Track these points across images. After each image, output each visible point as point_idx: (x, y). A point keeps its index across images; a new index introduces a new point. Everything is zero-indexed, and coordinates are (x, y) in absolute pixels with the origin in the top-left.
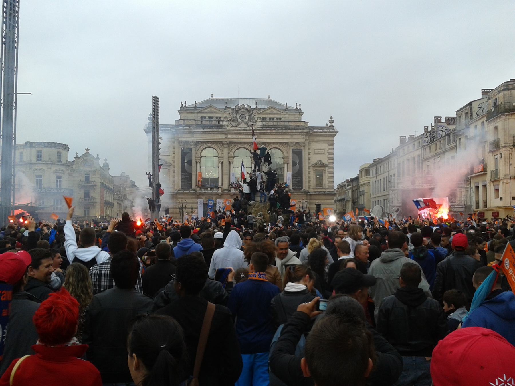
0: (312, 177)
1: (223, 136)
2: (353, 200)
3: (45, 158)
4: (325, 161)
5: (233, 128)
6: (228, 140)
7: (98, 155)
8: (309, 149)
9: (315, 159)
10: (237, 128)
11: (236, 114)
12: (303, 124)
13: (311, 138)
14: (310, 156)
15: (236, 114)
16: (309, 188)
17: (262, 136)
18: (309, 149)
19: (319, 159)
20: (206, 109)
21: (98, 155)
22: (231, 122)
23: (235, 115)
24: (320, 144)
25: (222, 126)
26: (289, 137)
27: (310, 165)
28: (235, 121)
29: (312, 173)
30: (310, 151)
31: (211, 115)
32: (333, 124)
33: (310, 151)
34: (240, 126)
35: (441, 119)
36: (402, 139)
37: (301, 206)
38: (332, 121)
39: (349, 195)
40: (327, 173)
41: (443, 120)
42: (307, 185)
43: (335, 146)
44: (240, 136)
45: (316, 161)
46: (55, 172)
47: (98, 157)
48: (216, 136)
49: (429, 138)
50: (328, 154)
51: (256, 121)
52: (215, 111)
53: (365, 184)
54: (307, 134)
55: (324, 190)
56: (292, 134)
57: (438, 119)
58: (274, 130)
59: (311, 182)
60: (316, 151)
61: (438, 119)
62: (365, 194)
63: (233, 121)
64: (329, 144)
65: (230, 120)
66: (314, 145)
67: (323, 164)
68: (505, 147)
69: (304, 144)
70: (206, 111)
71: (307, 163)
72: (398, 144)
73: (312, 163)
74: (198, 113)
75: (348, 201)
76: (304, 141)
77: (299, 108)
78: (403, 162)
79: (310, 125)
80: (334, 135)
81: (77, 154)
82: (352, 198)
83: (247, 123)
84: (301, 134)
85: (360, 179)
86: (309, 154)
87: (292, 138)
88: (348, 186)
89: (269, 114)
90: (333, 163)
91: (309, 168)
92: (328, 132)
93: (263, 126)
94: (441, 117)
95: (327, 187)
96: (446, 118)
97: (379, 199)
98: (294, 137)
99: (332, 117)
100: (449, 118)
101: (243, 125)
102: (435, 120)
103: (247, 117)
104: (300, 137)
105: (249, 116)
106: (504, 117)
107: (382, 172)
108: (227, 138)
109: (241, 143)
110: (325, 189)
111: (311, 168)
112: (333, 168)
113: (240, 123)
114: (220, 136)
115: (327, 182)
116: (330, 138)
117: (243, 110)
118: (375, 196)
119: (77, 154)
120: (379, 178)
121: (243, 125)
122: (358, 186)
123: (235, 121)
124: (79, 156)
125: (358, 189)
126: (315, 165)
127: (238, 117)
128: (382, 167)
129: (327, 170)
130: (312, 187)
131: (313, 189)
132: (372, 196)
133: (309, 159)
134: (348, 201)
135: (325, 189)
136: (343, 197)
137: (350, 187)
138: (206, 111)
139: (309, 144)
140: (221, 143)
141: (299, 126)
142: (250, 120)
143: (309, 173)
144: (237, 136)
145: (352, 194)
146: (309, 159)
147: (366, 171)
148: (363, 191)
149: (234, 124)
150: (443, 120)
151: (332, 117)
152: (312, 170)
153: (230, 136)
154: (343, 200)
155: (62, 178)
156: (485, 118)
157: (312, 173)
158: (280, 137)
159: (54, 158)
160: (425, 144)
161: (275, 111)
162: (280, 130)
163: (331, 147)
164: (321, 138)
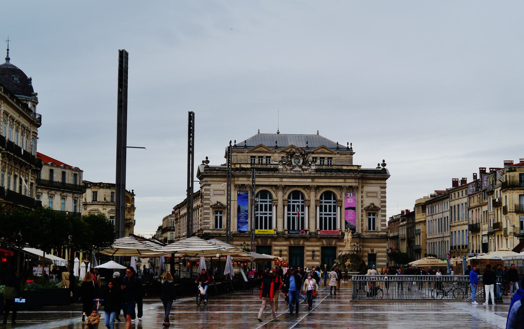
0: (364, 220)
1: (278, 180)
2: (408, 239)
3: (100, 198)
4: (377, 204)
5: (288, 172)
6: (283, 184)
7: (133, 191)
8: (362, 193)
9: (367, 202)
10: (292, 172)
11: (291, 158)
12: (356, 168)
13: (364, 181)
14: (363, 199)
15: (291, 158)
16: (362, 230)
17: (316, 180)
18: (362, 193)
19: (372, 202)
20: (256, 148)
21: (133, 191)
22: (286, 166)
23: (289, 159)
24: (372, 188)
25: (276, 170)
26: (342, 180)
27: (363, 208)
28: (290, 164)
29: (364, 216)
30: (363, 195)
31: (261, 155)
32: (385, 167)
33: (363, 195)
34: (295, 169)
35: (485, 170)
36: (455, 183)
37: (356, 249)
38: (384, 165)
39: (403, 232)
40: (379, 216)
41: (488, 171)
42: (360, 228)
43: (387, 190)
44: (295, 180)
45: (368, 205)
47: (133, 193)
48: (271, 180)
49: (474, 188)
50: (380, 197)
51: (310, 165)
52: (265, 150)
53: (420, 222)
54: (359, 178)
55: (377, 234)
56: (345, 178)
57: (482, 171)
58: (329, 174)
59: (364, 225)
60: (369, 194)
61: (482, 171)
62: (421, 233)
63: (288, 165)
64: (382, 188)
65: (285, 164)
66: (367, 189)
67: (376, 207)
68: (510, 212)
69: (357, 188)
70: (256, 150)
71: (360, 206)
72: (450, 186)
73: (365, 206)
74: (248, 153)
75: (403, 240)
76: (357, 184)
77: (350, 147)
78: (455, 206)
79: (362, 168)
82: (407, 236)
83: (300, 167)
84: (355, 178)
85: (416, 215)
86: (362, 197)
87: (345, 182)
88: (402, 221)
89: (320, 153)
90: (385, 206)
91: (362, 212)
92: (380, 175)
93: (317, 170)
94: (485, 168)
95: (380, 230)
96: (490, 169)
97: (435, 240)
98: (348, 181)
99: (384, 161)
100: (493, 169)
101: (297, 169)
102: (480, 171)
103: (301, 161)
104: (353, 181)
105: (303, 159)
106: (509, 191)
107: (437, 212)
108: (282, 181)
109: (295, 186)
110: (378, 232)
111: (364, 211)
112: (385, 211)
113: (294, 167)
114: (275, 180)
115: (380, 225)
116: (383, 182)
117: (297, 154)
118: (431, 237)
120: (435, 217)
121: (297, 169)
122: (414, 224)
123: (290, 164)
125: (414, 226)
126: (367, 209)
127: (293, 160)
128: (437, 206)
129: (380, 213)
130: (365, 229)
131: (366, 232)
132: (428, 237)
133: (362, 202)
134: (403, 240)
135: (378, 232)
136: (396, 234)
137: (405, 222)
138: (256, 150)
139: (362, 187)
140: (276, 187)
141: (352, 170)
142: (304, 163)
143: (362, 216)
144: (292, 180)
145: (407, 232)
146: (362, 202)
147: (422, 206)
148: (419, 230)
149: (288, 168)
150: (488, 171)
151: (384, 161)
152: (364, 213)
153: (284, 180)
154: (396, 238)
156: (500, 188)
157: (364, 216)
158: (334, 181)
159: (109, 199)
160: (471, 193)
161: (326, 151)
162: (334, 174)
163: (383, 190)
164: (373, 182)
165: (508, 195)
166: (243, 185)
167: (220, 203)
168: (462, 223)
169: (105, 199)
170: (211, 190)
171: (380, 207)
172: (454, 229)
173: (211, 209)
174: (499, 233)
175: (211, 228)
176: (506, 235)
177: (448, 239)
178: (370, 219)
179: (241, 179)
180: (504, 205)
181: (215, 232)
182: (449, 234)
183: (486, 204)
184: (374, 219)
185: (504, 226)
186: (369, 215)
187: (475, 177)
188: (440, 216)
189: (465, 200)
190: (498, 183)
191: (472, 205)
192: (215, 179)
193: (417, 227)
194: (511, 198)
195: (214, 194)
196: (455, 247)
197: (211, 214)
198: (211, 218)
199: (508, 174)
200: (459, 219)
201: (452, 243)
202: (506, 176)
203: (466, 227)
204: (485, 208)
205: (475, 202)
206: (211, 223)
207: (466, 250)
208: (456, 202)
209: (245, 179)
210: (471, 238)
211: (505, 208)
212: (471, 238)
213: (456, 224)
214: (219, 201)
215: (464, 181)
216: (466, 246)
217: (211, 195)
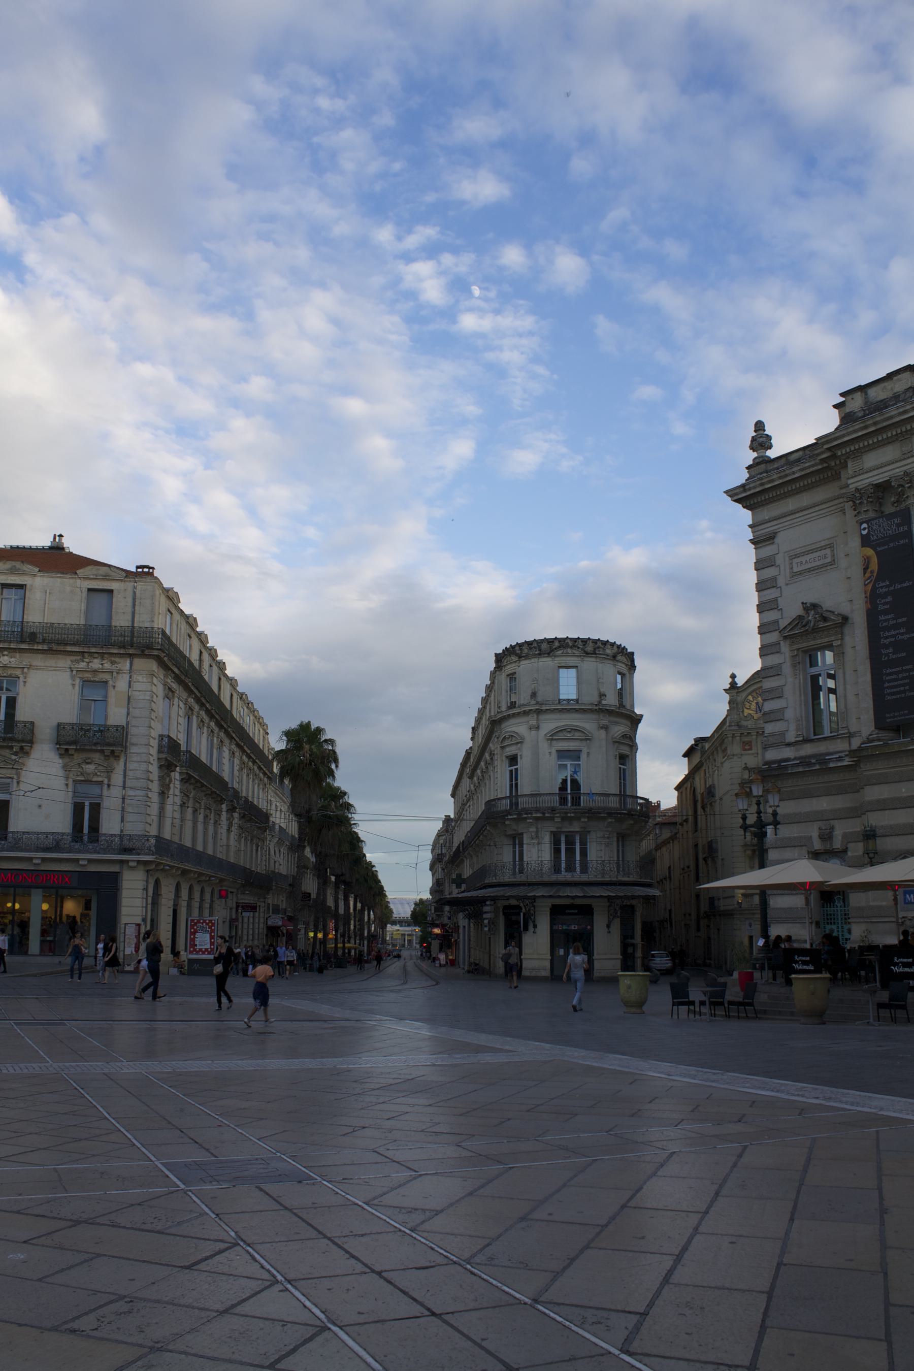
46: (552, 737)
81: (733, 676)
119: (733, 676)
124: (740, 681)
155: (583, 756)
166: (883, 488)
167: (814, 606)
169: (534, 695)
170: (779, 560)
173: (785, 647)
175: (791, 737)
179: (871, 459)
181: (808, 750)
192: (791, 504)
195: (794, 575)
197: (787, 669)
198: (788, 691)
206: (789, 714)
209: (889, 453)
214: (810, 599)
217: (781, 582)
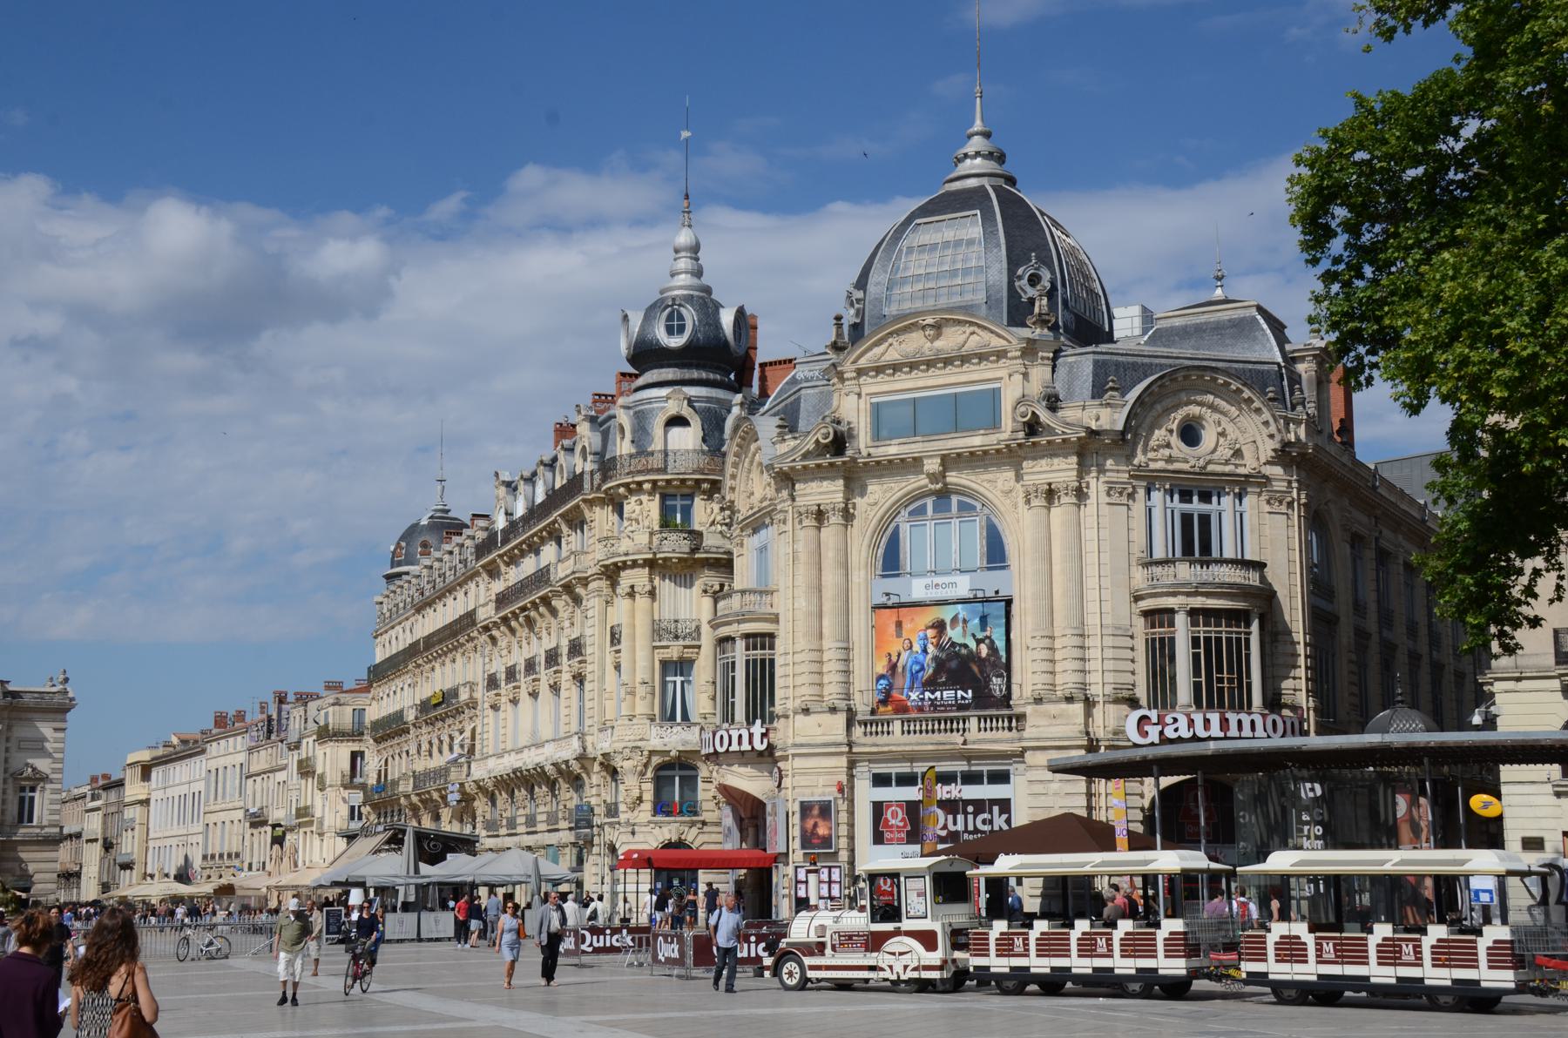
2: (105, 839)
8: (8, 740)
18: (8, 740)
29: (10, 791)
36: (221, 720)
40: (47, 795)
66: (20, 732)
73: (11, 770)
80: (68, 710)
88: (94, 798)
95: (45, 823)
97: (168, 842)
115: (46, 812)
120: (170, 793)
135: (42, 828)
148: (133, 820)
150: (291, 698)
157: (10, 791)
165: (328, 751)
168: (230, 806)
171: (48, 771)
172: (211, 819)
174: (308, 830)
176: (321, 835)
177: (200, 839)
178: (22, 799)
180: (319, 771)
182: (201, 829)
183: (283, 768)
184: (32, 799)
185: (318, 814)
186: (23, 789)
187: (263, 707)
188: (183, 790)
189: (241, 758)
190: (311, 725)
191: (254, 769)
193: (129, 813)
194: (333, 759)
196: (213, 857)
199: (331, 709)
200: (224, 797)
201: (206, 847)
202: (326, 714)
203: (240, 814)
204: (281, 776)
205: (261, 761)
207: (236, 863)
208: (221, 762)
210: (247, 836)
211: (322, 778)
212: (247, 836)
213: (218, 808)
215: (240, 716)
216: (237, 855)
